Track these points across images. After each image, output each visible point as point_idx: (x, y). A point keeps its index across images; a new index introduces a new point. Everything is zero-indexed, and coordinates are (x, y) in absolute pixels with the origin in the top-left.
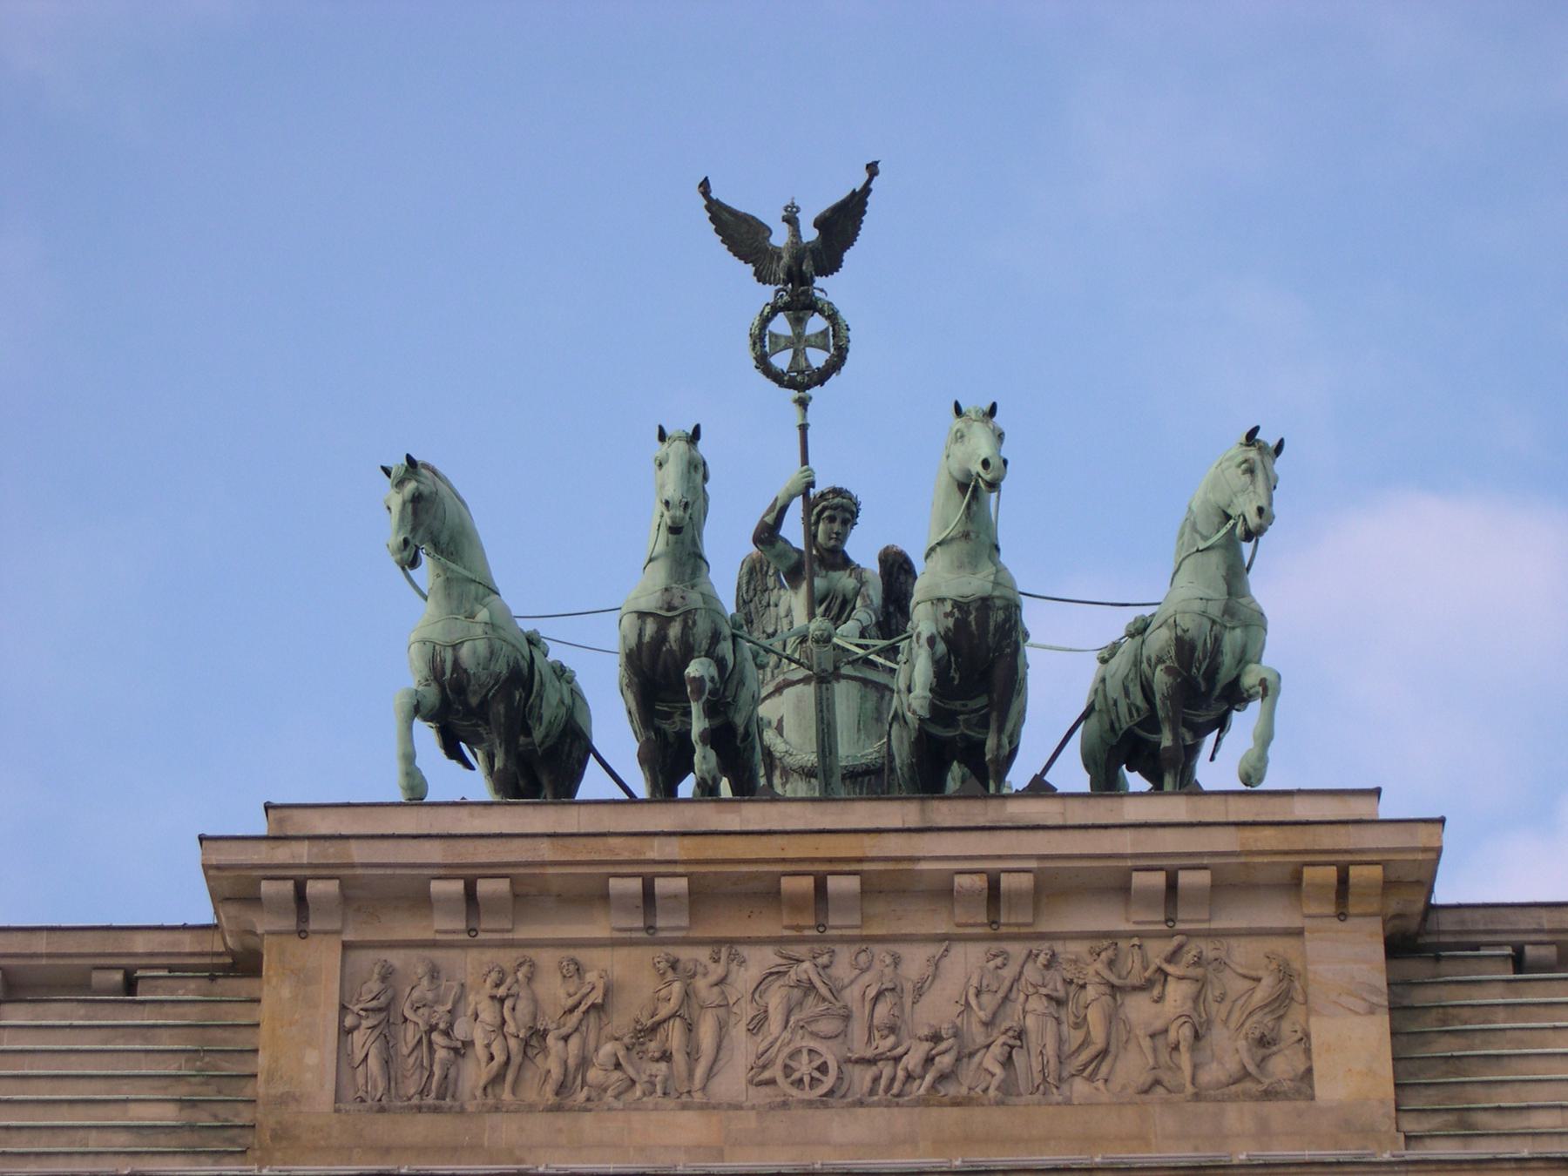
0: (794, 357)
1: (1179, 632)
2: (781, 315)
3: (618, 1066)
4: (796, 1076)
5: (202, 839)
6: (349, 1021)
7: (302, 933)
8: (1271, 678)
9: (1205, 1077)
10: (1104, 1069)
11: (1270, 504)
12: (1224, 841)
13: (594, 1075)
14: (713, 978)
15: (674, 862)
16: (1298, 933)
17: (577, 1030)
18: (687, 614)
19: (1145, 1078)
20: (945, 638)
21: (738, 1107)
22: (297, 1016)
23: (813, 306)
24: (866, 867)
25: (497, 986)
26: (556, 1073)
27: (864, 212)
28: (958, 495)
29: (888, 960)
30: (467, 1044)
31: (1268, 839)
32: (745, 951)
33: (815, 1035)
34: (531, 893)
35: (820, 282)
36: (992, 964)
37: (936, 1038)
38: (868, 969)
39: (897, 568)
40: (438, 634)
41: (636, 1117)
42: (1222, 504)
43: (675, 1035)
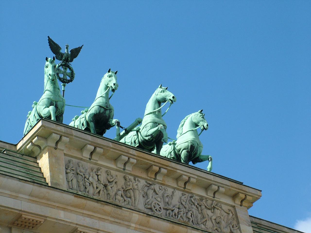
0: (64, 76)
3: (122, 196)
4: (156, 208)
6: (68, 171)
7: (56, 149)
10: (207, 223)
14: (136, 184)
15: (134, 155)
16: (234, 207)
19: (215, 228)
22: (57, 167)
23: (69, 67)
24: (168, 168)
27: (80, 52)
32: (139, 179)
33: (157, 200)
36: (184, 196)
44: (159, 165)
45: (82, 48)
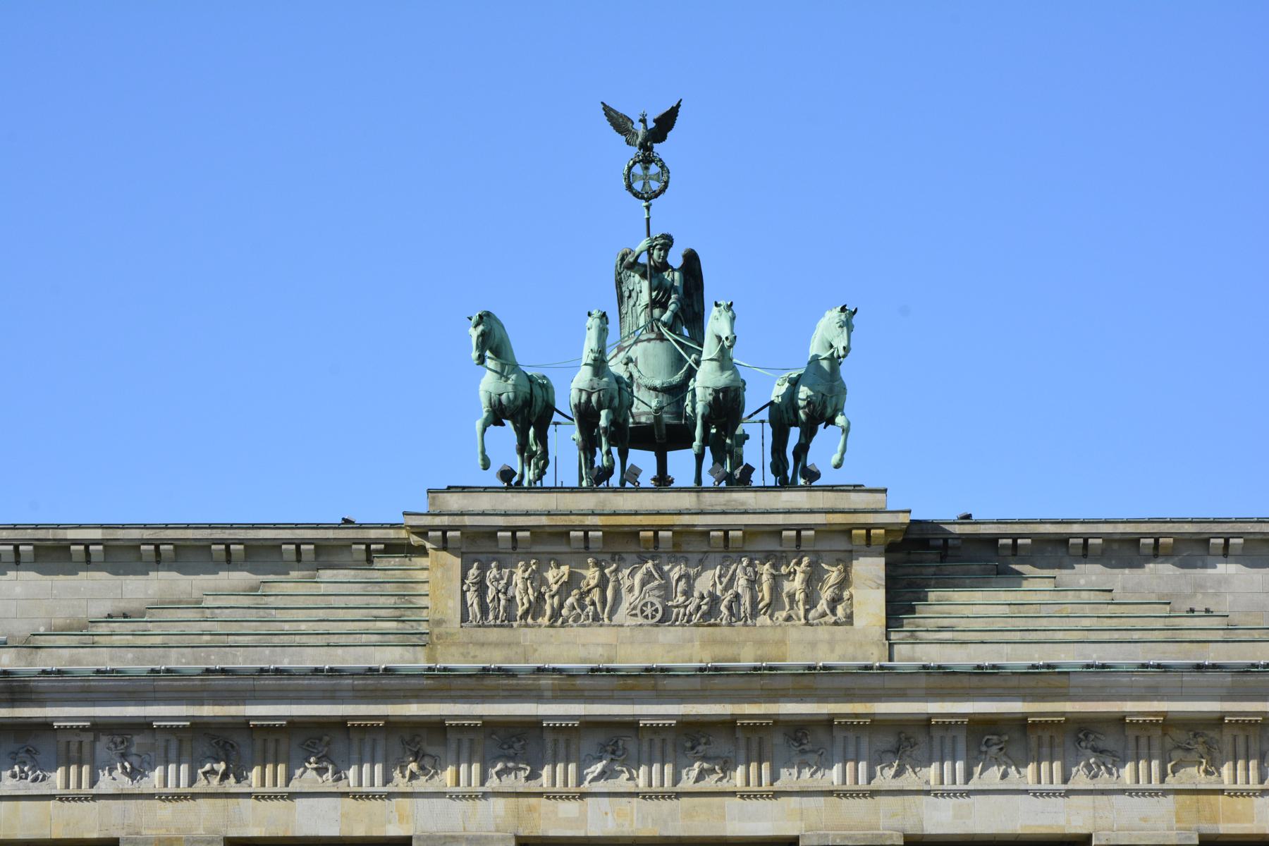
6: (465, 588)
9: (810, 616)
13: (564, 612)
17: (558, 592)
21: (622, 626)
25: (524, 571)
26: (548, 612)
28: (716, 340)
30: (514, 597)
32: (624, 556)
35: (657, 148)
37: (702, 598)
39: (691, 260)
41: (582, 629)
43: (596, 595)
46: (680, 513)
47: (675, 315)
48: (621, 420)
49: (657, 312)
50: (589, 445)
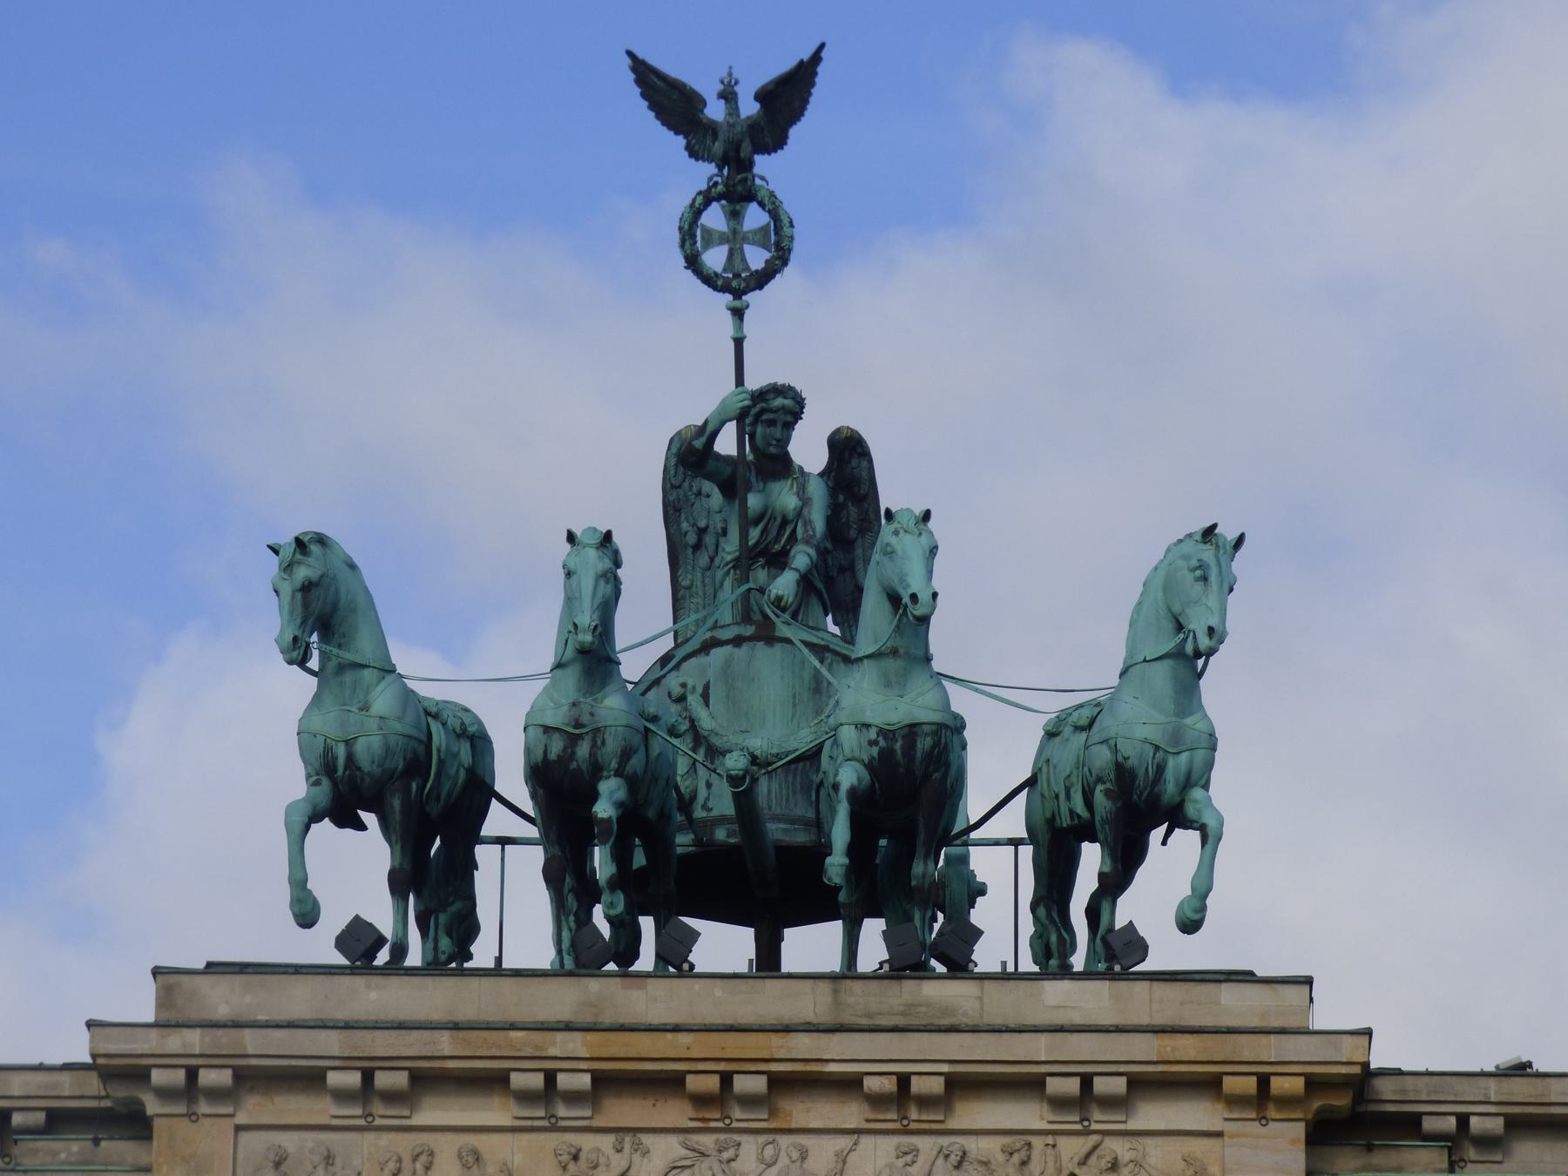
0: (731, 254)
1: (1120, 759)
2: (715, 204)
5: (90, 1024)
7: (192, 1116)
8: (1211, 823)
11: (1223, 620)
12: (1141, 1049)
16: (1218, 1135)
18: (598, 729)
20: (869, 766)
24: (774, 1067)
27: (813, 84)
28: (887, 606)
29: (795, 1155)
31: (1186, 1047)
32: (647, 1139)
34: (428, 1080)
38: (774, 1163)
39: (848, 451)
40: (333, 732)
42: (1177, 608)
44: (722, 1067)
45: (820, 59)
46: (787, 1029)
47: (805, 581)
48: (651, 813)
49: (760, 575)
50: (569, 884)
